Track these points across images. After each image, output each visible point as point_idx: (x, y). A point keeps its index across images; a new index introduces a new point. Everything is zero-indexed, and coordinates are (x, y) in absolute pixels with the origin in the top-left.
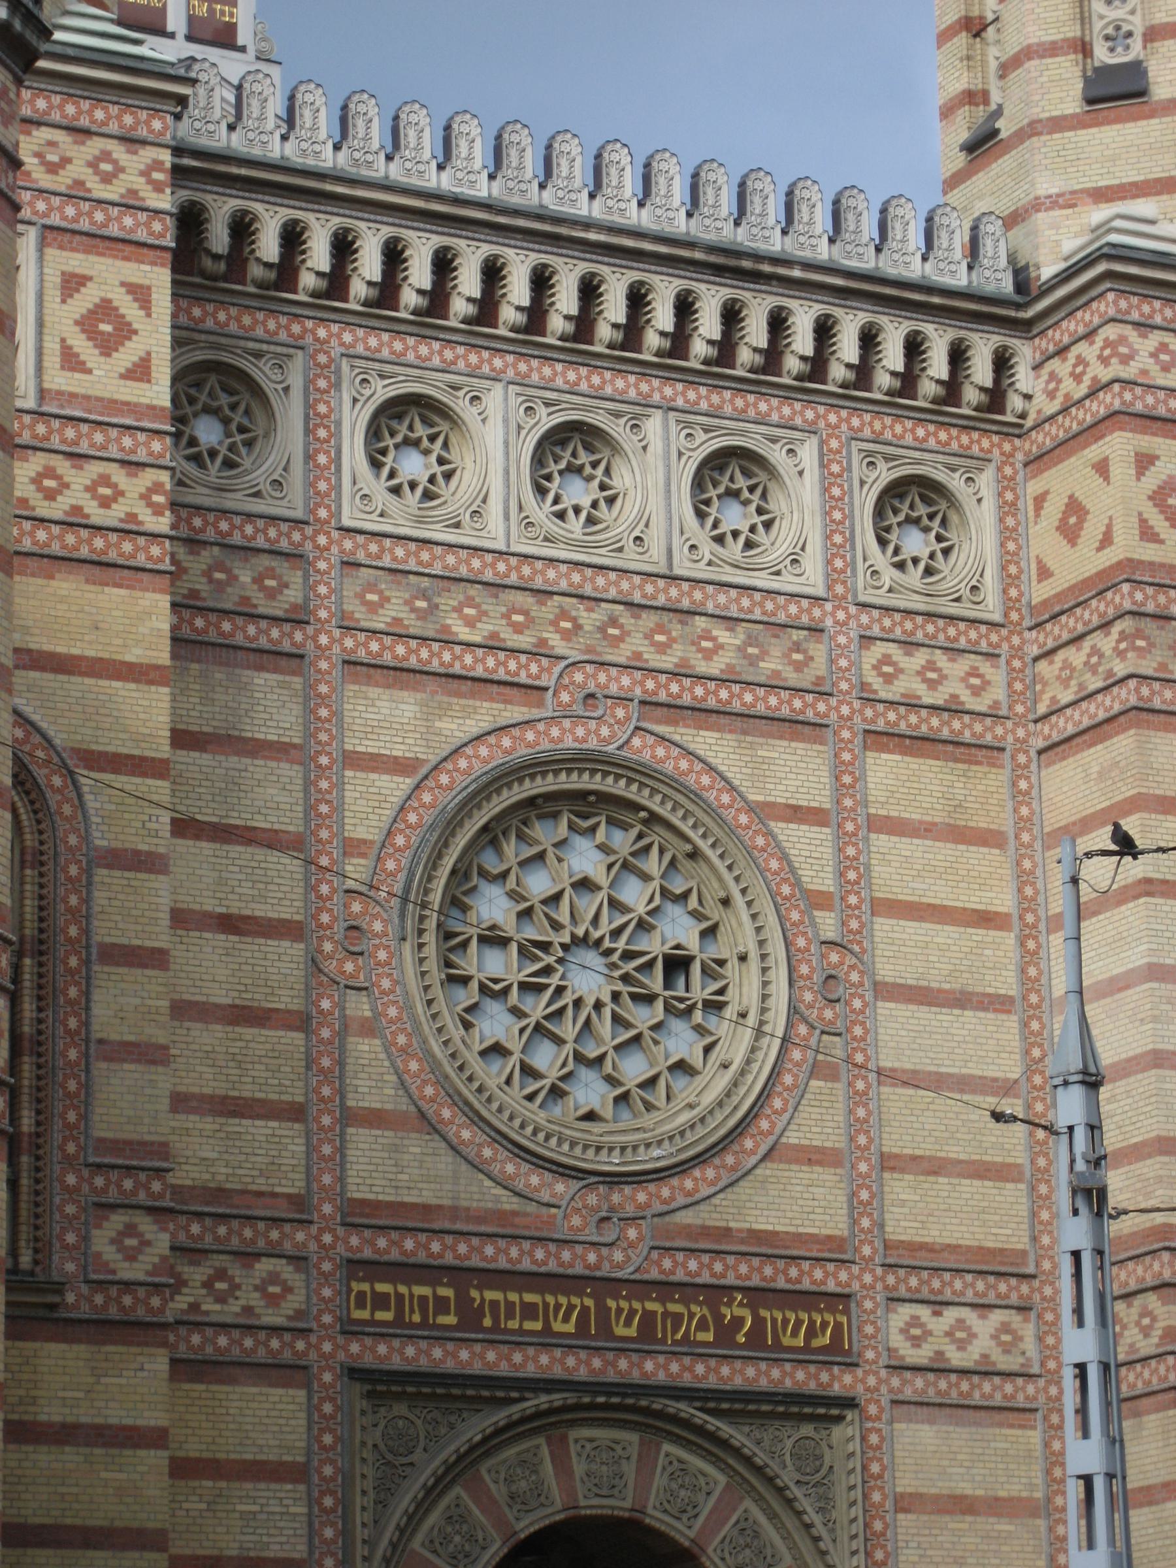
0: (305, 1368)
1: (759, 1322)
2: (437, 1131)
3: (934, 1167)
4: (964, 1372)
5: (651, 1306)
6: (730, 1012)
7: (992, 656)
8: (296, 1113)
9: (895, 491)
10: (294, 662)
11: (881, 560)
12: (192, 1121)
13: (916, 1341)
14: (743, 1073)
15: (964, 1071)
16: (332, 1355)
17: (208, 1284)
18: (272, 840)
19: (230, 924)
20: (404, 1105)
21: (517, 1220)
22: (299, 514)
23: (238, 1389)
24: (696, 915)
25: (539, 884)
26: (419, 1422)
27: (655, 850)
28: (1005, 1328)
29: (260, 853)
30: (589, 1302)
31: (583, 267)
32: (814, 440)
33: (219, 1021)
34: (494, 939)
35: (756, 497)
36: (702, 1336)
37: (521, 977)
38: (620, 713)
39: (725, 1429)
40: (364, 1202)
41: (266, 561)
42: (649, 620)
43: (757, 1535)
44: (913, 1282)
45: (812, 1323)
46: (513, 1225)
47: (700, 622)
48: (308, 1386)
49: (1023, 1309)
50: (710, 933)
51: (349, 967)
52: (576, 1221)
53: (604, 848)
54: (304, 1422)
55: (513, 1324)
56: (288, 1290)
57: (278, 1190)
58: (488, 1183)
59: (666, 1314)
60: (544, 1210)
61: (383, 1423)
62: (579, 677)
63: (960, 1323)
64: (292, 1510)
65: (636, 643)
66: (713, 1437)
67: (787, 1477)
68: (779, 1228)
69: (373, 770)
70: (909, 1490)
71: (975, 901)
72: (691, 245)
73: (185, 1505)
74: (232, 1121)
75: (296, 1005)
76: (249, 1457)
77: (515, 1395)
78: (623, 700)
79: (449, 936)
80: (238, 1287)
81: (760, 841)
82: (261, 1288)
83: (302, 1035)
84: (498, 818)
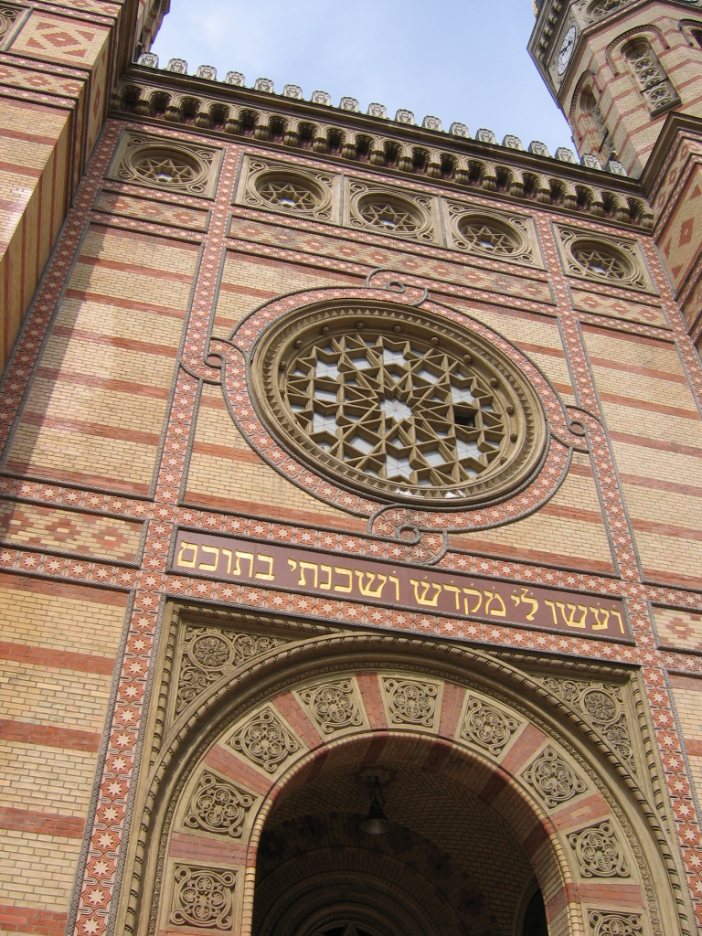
0: (127, 592)
1: (544, 610)
2: (268, 464)
3: (675, 532)
5: (447, 588)
6: (506, 440)
8: (150, 439)
10: (194, 246)
13: (683, 635)
14: (518, 462)
17: (51, 529)
18: (162, 311)
19: (119, 342)
20: (244, 447)
22: (210, 196)
23: (60, 599)
24: (475, 394)
25: (361, 366)
26: (231, 644)
27: (445, 361)
29: (151, 316)
30: (392, 579)
32: (531, 220)
33: (97, 385)
34: (324, 385)
36: (494, 613)
37: (345, 404)
38: (415, 293)
39: (521, 675)
41: (184, 210)
43: (561, 767)
44: (672, 597)
45: (591, 615)
50: (488, 402)
51: (209, 373)
52: (383, 527)
54: (120, 630)
55: (327, 587)
57: (125, 479)
59: (462, 596)
60: (357, 519)
62: (387, 276)
64: (93, 693)
66: (509, 681)
67: (585, 716)
68: (553, 552)
70: (696, 738)
71: (671, 404)
74: (95, 437)
75: (165, 385)
76: (62, 649)
79: (291, 378)
81: (517, 357)
82: (99, 537)
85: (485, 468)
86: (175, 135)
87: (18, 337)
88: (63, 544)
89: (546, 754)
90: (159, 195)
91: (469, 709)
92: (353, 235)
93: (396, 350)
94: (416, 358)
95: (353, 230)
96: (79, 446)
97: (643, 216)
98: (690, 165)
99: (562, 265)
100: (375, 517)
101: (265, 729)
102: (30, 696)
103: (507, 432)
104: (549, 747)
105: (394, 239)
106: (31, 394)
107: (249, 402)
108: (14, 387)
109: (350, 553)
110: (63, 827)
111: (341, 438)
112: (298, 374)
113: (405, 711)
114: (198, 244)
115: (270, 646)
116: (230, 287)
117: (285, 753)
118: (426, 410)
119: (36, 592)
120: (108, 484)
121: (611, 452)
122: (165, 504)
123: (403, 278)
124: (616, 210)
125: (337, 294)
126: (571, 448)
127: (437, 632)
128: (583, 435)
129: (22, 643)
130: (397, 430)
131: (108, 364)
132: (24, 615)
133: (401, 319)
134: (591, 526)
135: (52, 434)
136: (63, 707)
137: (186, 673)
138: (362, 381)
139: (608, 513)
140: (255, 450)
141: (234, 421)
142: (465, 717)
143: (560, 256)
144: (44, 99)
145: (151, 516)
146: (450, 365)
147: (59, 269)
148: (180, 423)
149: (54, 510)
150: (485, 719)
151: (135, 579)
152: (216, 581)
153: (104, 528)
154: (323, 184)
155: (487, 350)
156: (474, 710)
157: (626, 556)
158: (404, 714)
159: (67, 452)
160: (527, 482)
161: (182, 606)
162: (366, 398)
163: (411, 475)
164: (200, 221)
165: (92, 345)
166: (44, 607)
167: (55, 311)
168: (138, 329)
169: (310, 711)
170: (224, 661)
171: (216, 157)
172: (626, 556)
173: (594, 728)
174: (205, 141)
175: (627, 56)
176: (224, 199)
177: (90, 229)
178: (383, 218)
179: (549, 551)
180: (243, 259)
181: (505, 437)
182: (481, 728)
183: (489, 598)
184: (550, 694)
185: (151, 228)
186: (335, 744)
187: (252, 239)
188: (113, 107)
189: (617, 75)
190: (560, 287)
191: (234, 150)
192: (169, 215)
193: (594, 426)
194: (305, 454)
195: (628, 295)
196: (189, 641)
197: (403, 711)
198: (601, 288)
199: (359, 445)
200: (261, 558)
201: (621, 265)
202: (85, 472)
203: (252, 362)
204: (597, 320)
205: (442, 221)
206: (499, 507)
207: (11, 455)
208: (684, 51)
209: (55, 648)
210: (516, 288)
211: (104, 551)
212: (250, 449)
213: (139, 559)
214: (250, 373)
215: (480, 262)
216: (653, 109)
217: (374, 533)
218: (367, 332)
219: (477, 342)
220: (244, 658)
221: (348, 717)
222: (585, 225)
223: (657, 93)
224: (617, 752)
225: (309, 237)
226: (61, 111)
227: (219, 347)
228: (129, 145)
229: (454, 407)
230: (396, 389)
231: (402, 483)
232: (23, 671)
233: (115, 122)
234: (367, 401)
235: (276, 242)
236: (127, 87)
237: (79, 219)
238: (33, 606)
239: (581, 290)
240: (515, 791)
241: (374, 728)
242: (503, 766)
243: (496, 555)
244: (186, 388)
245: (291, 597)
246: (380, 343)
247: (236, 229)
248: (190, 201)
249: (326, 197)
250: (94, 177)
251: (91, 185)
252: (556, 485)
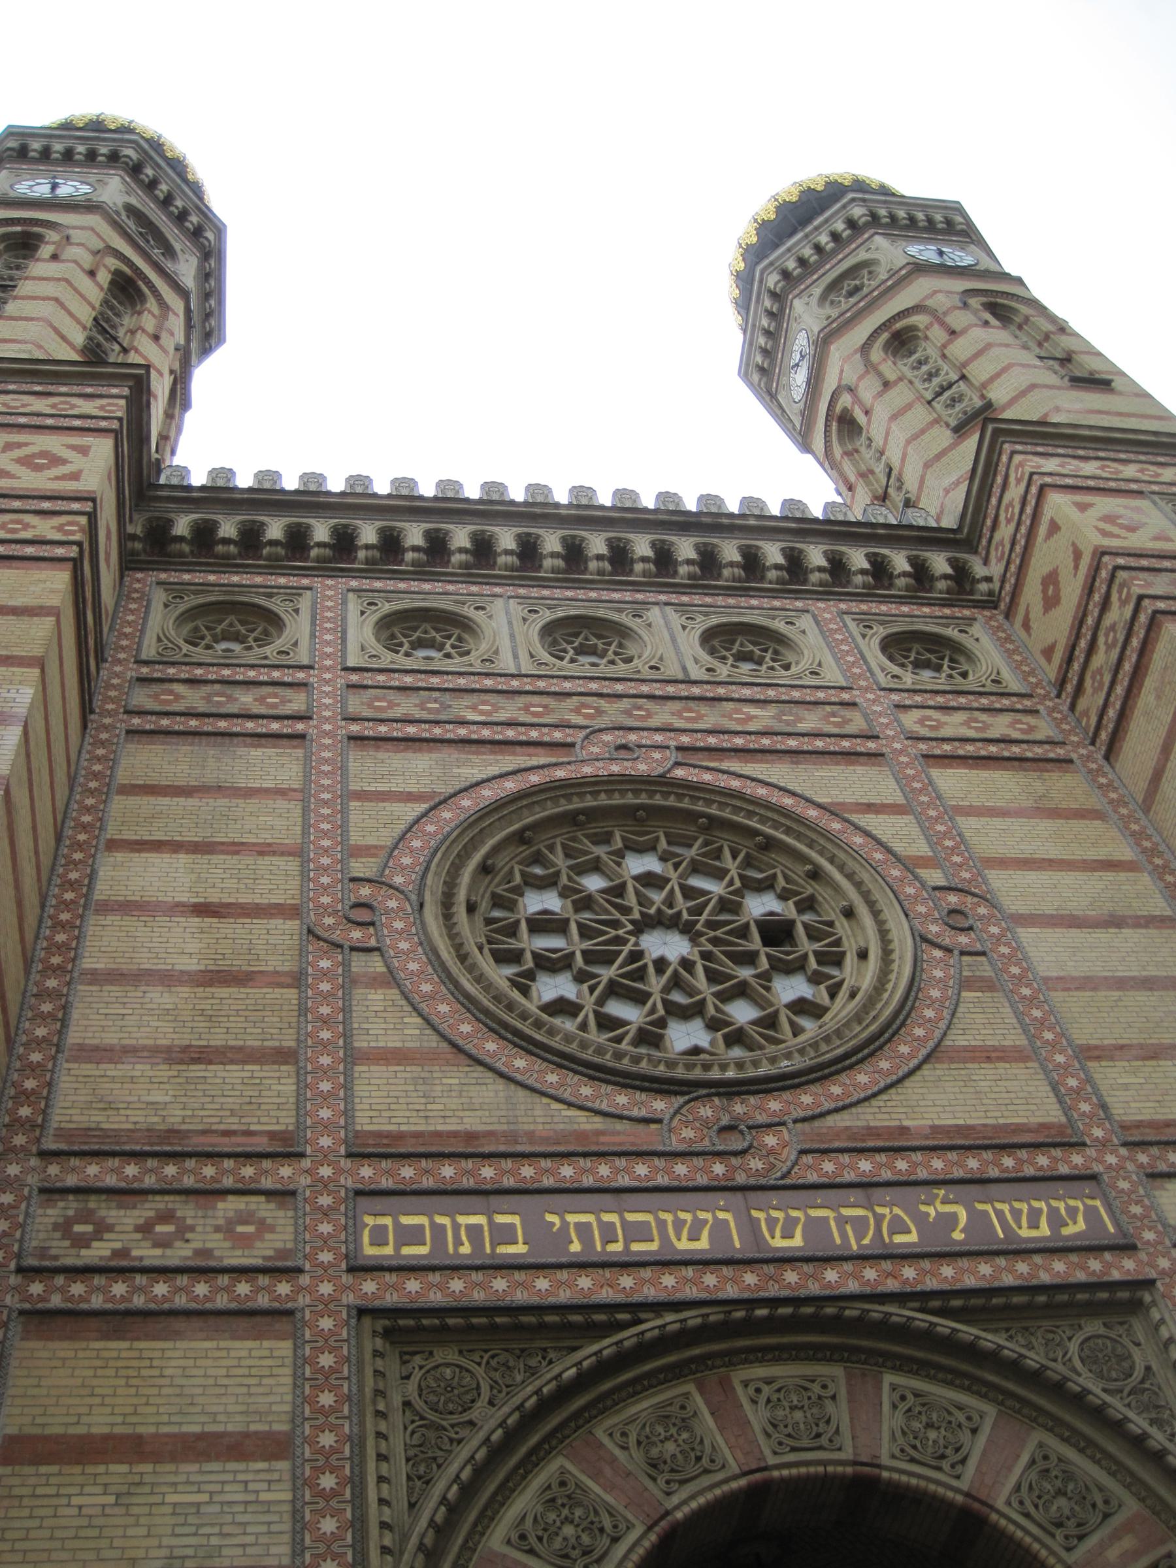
0: (290, 1313)
2: (480, 1063)
5: (814, 1213)
6: (850, 960)
7: (1033, 712)
8: (282, 1056)
10: (295, 742)
12: (140, 1069)
15: (1144, 973)
16: (332, 1299)
17: (145, 1229)
18: (264, 850)
19: (203, 910)
20: (432, 1041)
21: (602, 1139)
22: (305, 662)
23: (179, 1344)
24: (783, 897)
25: (594, 883)
26: (480, 1371)
27: (727, 853)
29: (248, 860)
30: (721, 1215)
32: (808, 616)
33: (181, 983)
35: (769, 655)
36: (899, 1239)
38: (657, 755)
39: (967, 1331)
40: (379, 1135)
41: (270, 689)
42: (677, 706)
43: (1068, 1476)
45: (1053, 1213)
46: (597, 1144)
47: (731, 705)
48: (295, 1337)
50: (808, 904)
51: (357, 934)
52: (688, 1133)
54: (289, 1380)
56: (264, 1227)
57: (253, 1128)
58: (556, 1106)
59: (842, 1221)
61: (417, 1375)
62: (607, 737)
64: (263, 1497)
66: (950, 1345)
68: (970, 1122)
69: (383, 801)
71: (1092, 855)
73: (75, 1501)
74: (192, 1067)
75: (287, 965)
76: (196, 1429)
77: (623, 1316)
79: (489, 921)
80: (192, 1229)
81: (836, 826)
82: (227, 1230)
83: (295, 991)
84: (533, 827)
85: (826, 1009)
86: (235, 579)
87: (39, 927)
88: (169, 1252)
89: (1038, 1458)
90: (226, 672)
91: (895, 1407)
92: (541, 684)
93: (641, 850)
94: (678, 855)
95: (540, 677)
96: (167, 1086)
97: (975, 581)
98: (1034, 490)
99: (872, 674)
100: (671, 1119)
101: (563, 1505)
102: (158, 1520)
103: (850, 947)
104: (1041, 1445)
105: (605, 679)
106: (75, 1014)
107: (431, 971)
108: (46, 1007)
109: (645, 1184)
111: (589, 1003)
112: (496, 914)
113: (790, 1430)
114: (302, 737)
115: (544, 1363)
116: (362, 796)
117: (606, 1541)
118: (712, 934)
119: (138, 1339)
120: (226, 1140)
121: (1019, 947)
122: (325, 1157)
123: (633, 737)
124: (932, 579)
125: (534, 778)
126: (956, 952)
127: (814, 1288)
128: (971, 928)
129: (128, 1430)
130: (676, 973)
131: (193, 946)
132: (122, 1382)
133: (643, 799)
134: (1017, 1069)
135: (120, 1073)
136: (216, 1530)
137: (413, 1433)
138: (601, 906)
139: (1039, 1044)
140: (454, 1045)
141: (412, 1004)
142: (891, 1421)
143: (866, 662)
144: (30, 550)
145: (305, 1180)
146: (734, 857)
147: (88, 810)
148: (325, 1021)
149: (143, 1198)
150: (924, 1418)
151: (300, 1289)
152: (433, 1269)
153: (231, 1214)
154: (478, 616)
155: (788, 823)
156: (903, 1407)
157: (1085, 1107)
158: (789, 1435)
159: (151, 1099)
160: (901, 1017)
161: (387, 1322)
162: (613, 933)
163: (713, 1043)
164: (297, 702)
165: (162, 920)
166: (155, 1363)
167: (92, 876)
168: (231, 884)
169: (632, 1460)
170: (473, 1401)
171: (305, 603)
172: (1085, 1107)
173: (1108, 1398)
174: (282, 581)
175: (895, 354)
176: (328, 663)
177: (126, 740)
178: (581, 651)
179: (961, 1122)
180: (377, 748)
181: (848, 955)
182: (921, 1435)
183: (884, 1216)
184: (1021, 1355)
185: (223, 724)
186: (686, 1509)
187: (384, 716)
188: (133, 553)
189: (886, 385)
190: (878, 709)
191: (330, 588)
192: (246, 699)
193: (982, 911)
194: (538, 1037)
195: (984, 701)
196: (408, 1377)
197: (787, 1431)
198: (940, 699)
199: (617, 1009)
200: (501, 1219)
201: (962, 659)
202: (184, 1127)
203: (422, 905)
204: (947, 748)
205: (673, 639)
206: (866, 1066)
207: (57, 1118)
208: (979, 335)
209: (186, 1429)
210: (810, 721)
211: (239, 1253)
212: (445, 1045)
213: (300, 1255)
214: (423, 923)
215: (747, 692)
216: (953, 423)
217: (675, 1145)
218: (594, 828)
219: (769, 814)
220: (505, 1390)
221: (698, 1459)
222: (893, 608)
223: (953, 400)
224: (1153, 1431)
225: (475, 698)
226: (58, 565)
227: (365, 891)
228: (166, 606)
229: (757, 922)
230: (659, 911)
231: (702, 1056)
232: (137, 1479)
233: (139, 575)
234: (617, 937)
235: (425, 715)
236: (149, 520)
237: (106, 728)
238: (135, 1363)
239: (910, 707)
240: (1002, 1533)
241: (746, 1468)
242: (974, 1493)
243: (880, 1144)
244: (325, 964)
245: (563, 1275)
246: (618, 843)
247: (356, 704)
248: (276, 674)
249: (488, 632)
250: (119, 662)
251: (117, 675)
252: (946, 1014)
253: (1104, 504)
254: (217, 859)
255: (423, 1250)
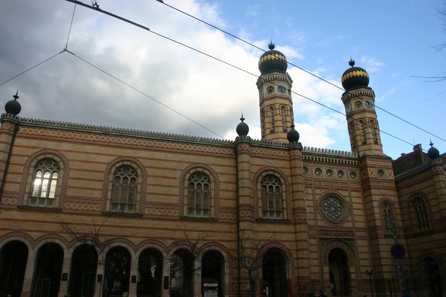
3: (358, 222)
4: (362, 236)
9: (351, 172)
11: (351, 178)
18: (311, 200)
28: (364, 233)
31: (328, 158)
34: (326, 206)
41: (309, 181)
42: (335, 183)
49: (366, 232)
53: (333, 200)
63: (361, 233)
65: (334, 185)
66: (345, 242)
67: (350, 245)
71: (360, 202)
72: (336, 156)
78: (334, 189)
103: (343, 210)
110: (317, 259)
154: (321, 169)
253: (372, 169)
254: (309, 201)
255: (321, 234)
